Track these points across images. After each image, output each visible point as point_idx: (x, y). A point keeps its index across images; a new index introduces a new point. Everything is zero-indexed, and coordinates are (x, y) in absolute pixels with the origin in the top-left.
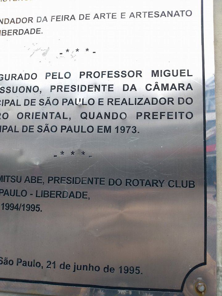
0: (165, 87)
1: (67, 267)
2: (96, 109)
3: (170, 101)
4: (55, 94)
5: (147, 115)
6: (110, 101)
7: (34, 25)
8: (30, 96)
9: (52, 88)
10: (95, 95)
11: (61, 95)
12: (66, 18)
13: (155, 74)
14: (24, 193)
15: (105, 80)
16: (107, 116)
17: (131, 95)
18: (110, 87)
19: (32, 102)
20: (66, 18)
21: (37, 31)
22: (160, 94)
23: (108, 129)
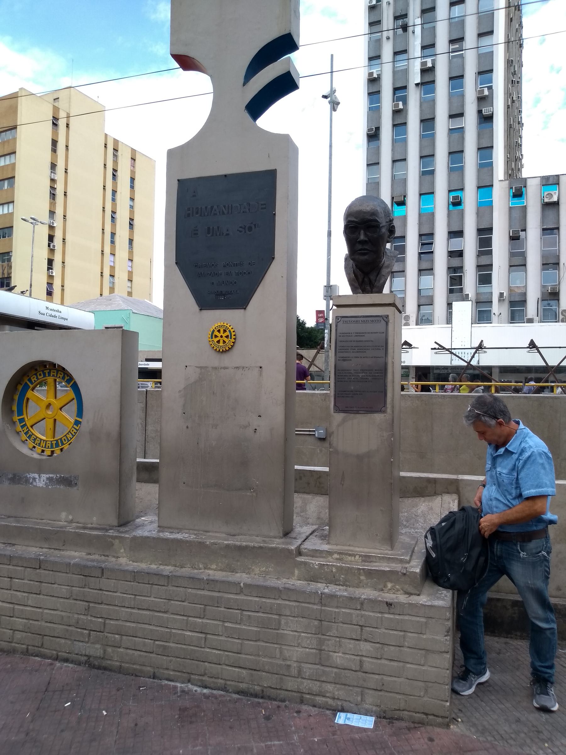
0: (378, 373)
1: (359, 407)
2: (364, 377)
3: (378, 376)
4: (355, 374)
5: (374, 379)
6: (366, 376)
7: (350, 359)
8: (350, 374)
9: (355, 373)
10: (364, 374)
11: (357, 374)
12: (357, 357)
13: (375, 370)
14: (350, 394)
15: (366, 372)
16: (366, 379)
17: (371, 375)
18: (367, 373)
19: (350, 376)
20: (357, 357)
21: (351, 360)
22: (377, 375)
23: (366, 381)
